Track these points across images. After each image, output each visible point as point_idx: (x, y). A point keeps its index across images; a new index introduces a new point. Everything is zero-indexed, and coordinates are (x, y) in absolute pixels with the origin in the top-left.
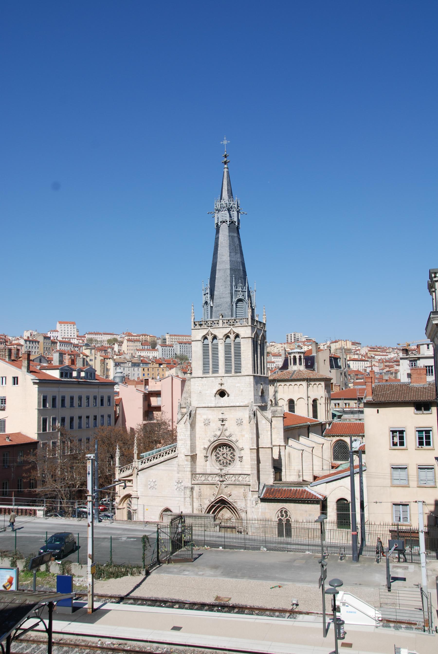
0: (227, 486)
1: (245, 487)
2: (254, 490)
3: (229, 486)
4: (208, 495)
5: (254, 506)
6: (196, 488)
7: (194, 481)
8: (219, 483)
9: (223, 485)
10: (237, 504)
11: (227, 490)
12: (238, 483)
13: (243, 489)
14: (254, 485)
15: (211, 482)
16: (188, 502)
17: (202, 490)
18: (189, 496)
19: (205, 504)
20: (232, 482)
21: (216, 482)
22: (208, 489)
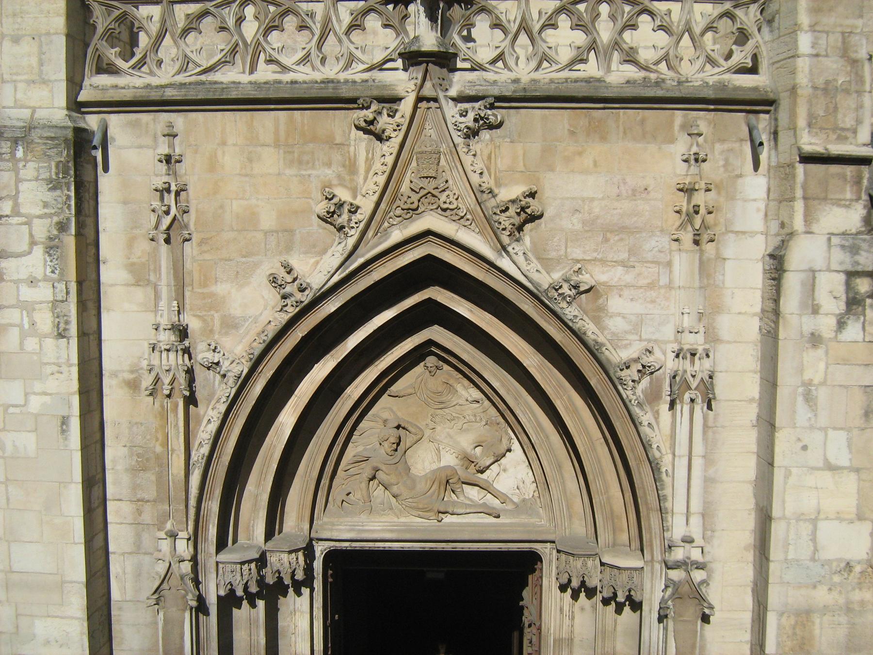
0: (493, 108)
1: (703, 120)
2: (837, 149)
3: (513, 118)
4: (268, 220)
5: (826, 324)
6: (132, 150)
7: (104, 80)
8: (402, 81)
9: (451, 110)
10: (598, 315)
11: (504, 161)
12: (620, 75)
13: (681, 146)
14: (827, 90)
15: (305, 74)
16: (28, 307)
17: (191, 171)
18: (42, 229)
19: (230, 325)
20: (548, 77)
21: (356, 73)
22: (270, 161)
